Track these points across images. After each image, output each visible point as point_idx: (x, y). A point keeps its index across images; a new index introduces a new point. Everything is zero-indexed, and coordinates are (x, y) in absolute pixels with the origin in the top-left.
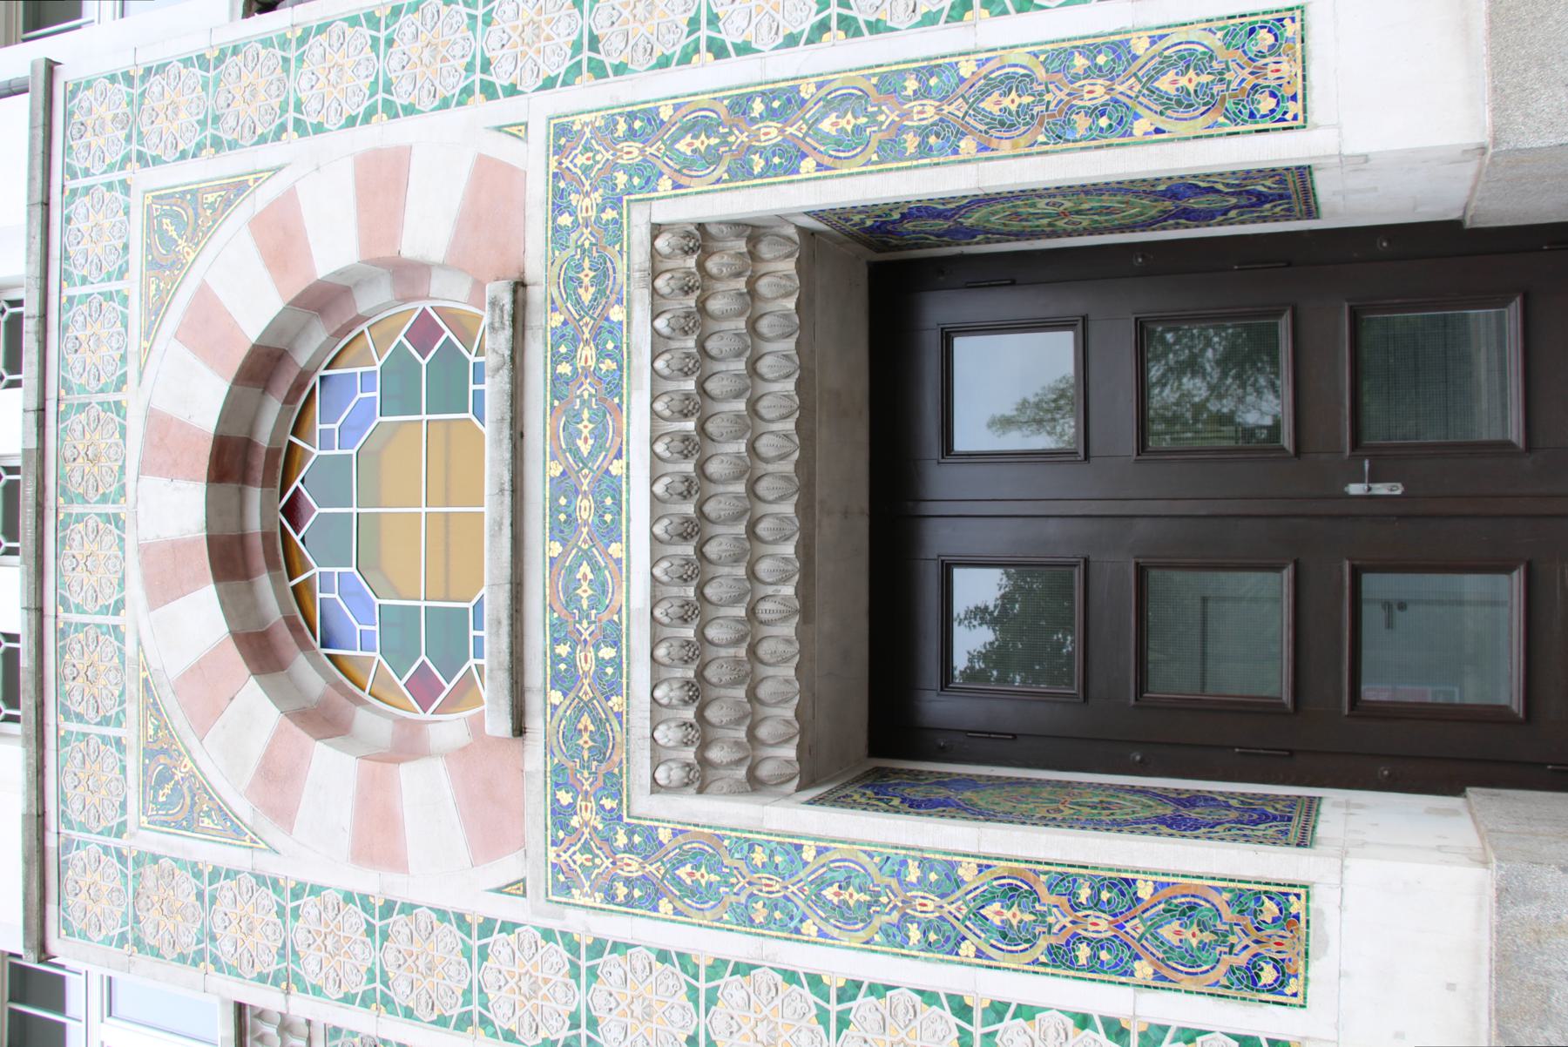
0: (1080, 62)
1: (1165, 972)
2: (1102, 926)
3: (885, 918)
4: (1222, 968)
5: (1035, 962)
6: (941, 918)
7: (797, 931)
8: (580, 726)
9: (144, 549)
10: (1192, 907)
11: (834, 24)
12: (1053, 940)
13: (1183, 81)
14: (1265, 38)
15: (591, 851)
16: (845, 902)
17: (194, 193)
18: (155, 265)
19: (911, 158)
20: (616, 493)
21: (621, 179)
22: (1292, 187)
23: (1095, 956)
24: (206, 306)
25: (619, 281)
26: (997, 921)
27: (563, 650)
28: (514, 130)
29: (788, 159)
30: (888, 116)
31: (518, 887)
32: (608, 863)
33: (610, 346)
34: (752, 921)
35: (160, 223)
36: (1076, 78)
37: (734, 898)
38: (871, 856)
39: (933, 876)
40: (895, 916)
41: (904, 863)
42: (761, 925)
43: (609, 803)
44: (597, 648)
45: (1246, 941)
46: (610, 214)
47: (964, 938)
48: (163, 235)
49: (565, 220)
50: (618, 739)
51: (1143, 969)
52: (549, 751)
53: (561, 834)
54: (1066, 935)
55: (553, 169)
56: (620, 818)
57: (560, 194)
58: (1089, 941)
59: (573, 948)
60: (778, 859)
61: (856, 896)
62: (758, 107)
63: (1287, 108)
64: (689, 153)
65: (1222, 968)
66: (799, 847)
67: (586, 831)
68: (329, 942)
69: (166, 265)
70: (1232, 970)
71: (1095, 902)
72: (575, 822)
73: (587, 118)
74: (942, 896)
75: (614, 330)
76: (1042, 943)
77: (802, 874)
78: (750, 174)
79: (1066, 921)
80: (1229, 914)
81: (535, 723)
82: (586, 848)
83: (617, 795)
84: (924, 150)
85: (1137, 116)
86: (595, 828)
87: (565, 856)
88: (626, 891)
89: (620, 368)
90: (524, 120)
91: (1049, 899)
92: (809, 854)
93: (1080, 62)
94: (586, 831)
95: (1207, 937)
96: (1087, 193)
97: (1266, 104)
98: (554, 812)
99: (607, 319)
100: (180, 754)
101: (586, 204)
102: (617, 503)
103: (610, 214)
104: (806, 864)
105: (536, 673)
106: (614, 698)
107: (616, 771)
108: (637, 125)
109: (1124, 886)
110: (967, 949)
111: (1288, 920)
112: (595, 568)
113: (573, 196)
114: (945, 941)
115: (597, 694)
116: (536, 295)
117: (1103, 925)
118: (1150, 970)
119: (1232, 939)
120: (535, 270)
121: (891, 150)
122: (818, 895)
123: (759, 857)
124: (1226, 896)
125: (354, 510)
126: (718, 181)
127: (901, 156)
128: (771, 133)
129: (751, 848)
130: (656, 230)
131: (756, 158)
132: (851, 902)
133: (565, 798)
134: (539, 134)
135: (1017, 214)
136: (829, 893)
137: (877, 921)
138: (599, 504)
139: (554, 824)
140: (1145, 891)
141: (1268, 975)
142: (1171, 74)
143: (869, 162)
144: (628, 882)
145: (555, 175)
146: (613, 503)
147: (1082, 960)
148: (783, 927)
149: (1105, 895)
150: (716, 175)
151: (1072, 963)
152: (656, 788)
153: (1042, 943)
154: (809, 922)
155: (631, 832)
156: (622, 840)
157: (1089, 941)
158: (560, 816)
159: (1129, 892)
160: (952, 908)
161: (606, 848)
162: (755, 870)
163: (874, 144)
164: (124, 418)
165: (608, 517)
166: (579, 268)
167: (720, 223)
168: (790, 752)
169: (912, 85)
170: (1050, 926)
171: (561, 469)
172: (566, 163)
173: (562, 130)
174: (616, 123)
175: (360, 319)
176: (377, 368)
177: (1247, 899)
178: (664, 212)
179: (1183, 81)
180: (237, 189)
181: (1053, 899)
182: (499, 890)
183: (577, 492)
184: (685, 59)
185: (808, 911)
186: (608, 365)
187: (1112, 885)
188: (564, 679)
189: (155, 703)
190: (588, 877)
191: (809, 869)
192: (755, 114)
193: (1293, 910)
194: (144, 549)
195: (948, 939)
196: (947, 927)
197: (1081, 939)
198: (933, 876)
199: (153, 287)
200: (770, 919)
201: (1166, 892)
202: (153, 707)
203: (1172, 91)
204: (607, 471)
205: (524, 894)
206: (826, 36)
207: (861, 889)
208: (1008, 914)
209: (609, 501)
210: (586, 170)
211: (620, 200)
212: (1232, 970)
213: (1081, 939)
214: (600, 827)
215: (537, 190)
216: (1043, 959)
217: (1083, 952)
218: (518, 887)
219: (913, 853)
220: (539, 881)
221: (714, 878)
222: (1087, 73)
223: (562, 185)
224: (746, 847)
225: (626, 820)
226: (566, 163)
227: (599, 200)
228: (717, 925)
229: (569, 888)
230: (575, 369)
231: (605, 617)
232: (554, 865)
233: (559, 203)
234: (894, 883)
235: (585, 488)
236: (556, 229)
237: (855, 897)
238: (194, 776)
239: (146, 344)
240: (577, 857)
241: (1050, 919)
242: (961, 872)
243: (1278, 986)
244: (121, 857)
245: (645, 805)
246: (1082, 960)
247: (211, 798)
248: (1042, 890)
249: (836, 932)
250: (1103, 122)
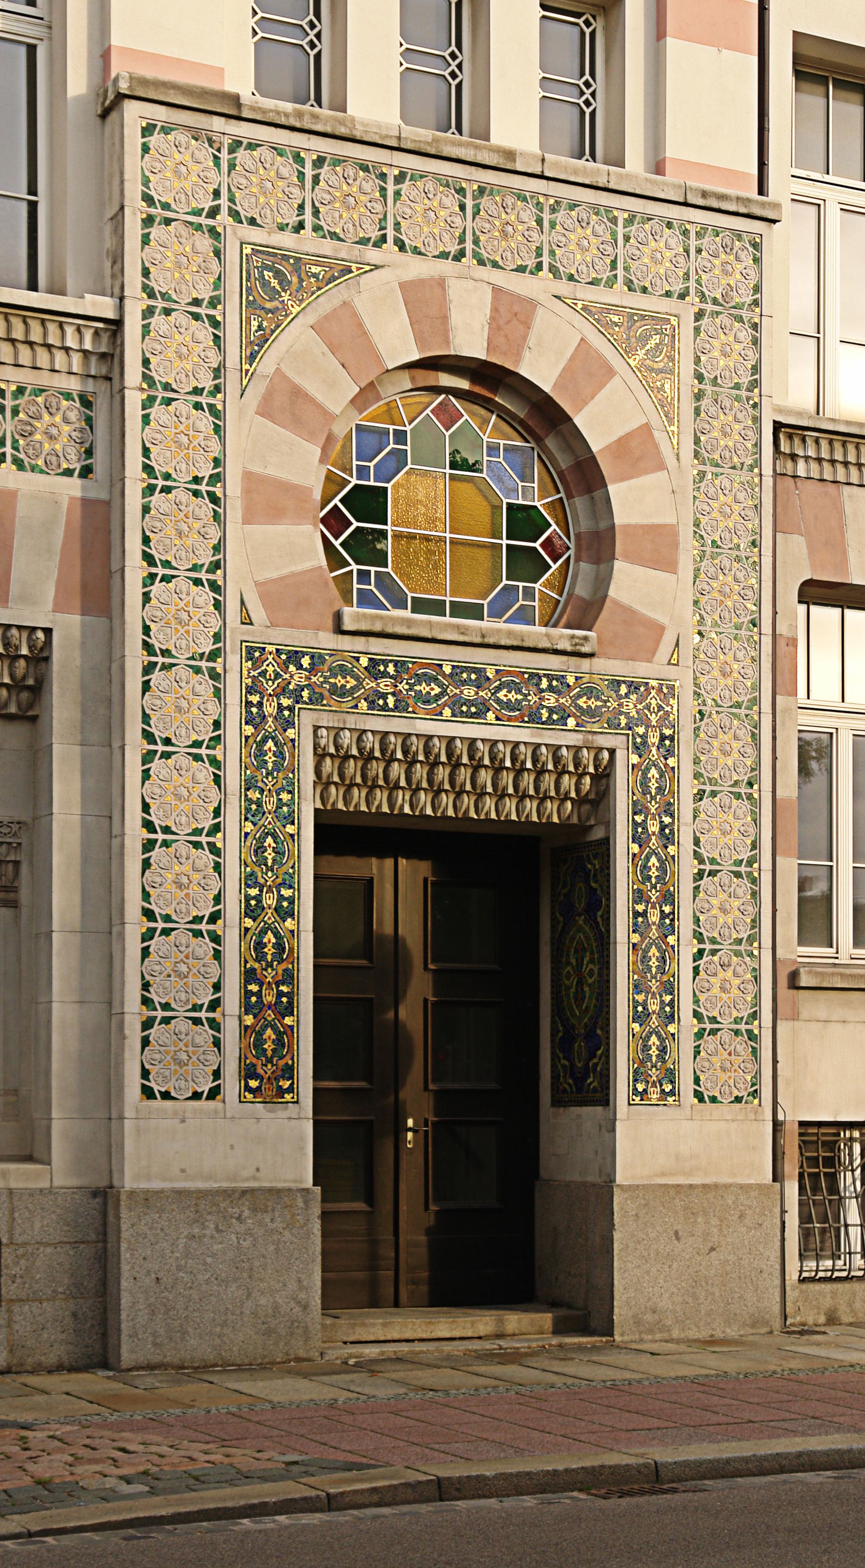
1: (249, 1031)
2: (269, 998)
3: (260, 874)
4: (254, 1061)
5: (246, 962)
6: (264, 908)
7: (246, 819)
10: (283, 1045)
11: (702, 867)
12: (259, 971)
13: (654, 1048)
14: (668, 1088)
15: (276, 679)
16: (266, 850)
17: (672, 372)
19: (634, 908)
21: (641, 730)
23: (253, 994)
25: (588, 725)
26: (265, 940)
27: (391, 669)
28: (675, 656)
29: (639, 837)
30: (654, 896)
32: (270, 691)
33: (555, 717)
34: (247, 789)
36: (661, 996)
37: (260, 778)
38: (293, 867)
39: (285, 904)
40: (262, 881)
41: (291, 887)
42: (246, 795)
43: (305, 693)
44: (393, 694)
45: (269, 1072)
46: (623, 721)
47: (254, 920)
49: (623, 689)
50: (343, 705)
51: (249, 1020)
52: (334, 652)
53: (284, 657)
54: (263, 978)
56: (298, 702)
58: (260, 991)
59: (213, 656)
60: (285, 809)
61: (270, 857)
65: (254, 1061)
66: (293, 823)
67: (287, 676)
68: (184, 439)
70: (254, 1065)
71: (280, 994)
72: (292, 668)
73: (675, 709)
74: (275, 909)
75: (563, 720)
76: (257, 965)
77: (278, 824)
78: (635, 813)
79: (269, 979)
80: (282, 1063)
81: (346, 643)
82: (277, 675)
83: (311, 701)
84: (637, 914)
85: (641, 1025)
86: (289, 683)
87: (270, 657)
88: (255, 702)
89: (543, 723)
91: (280, 969)
92: (290, 829)
93: (667, 998)
94: (287, 676)
95: (269, 1053)
96: (600, 994)
97: (640, 1087)
98: (296, 652)
99: (569, 716)
100: (301, 301)
102: (473, 715)
103: (623, 721)
104: (284, 826)
105: (377, 646)
106: (365, 704)
107: (325, 702)
108: (667, 742)
109: (290, 1010)
110: (249, 923)
111: (281, 1092)
112: (438, 697)
114: (252, 910)
115: (367, 693)
116: (585, 664)
117: (269, 999)
118: (249, 1023)
119: (269, 1066)
120: (600, 664)
121: (639, 896)
122: (267, 834)
123: (285, 797)
124: (290, 1062)
126: (633, 794)
127: (635, 902)
128: (654, 827)
129: (290, 792)
130: (612, 752)
131: (642, 818)
132: (266, 854)
133: (306, 662)
134: (671, 672)
135: (584, 950)
136: (269, 840)
137: (257, 869)
138: (469, 703)
139: (289, 651)
140: (288, 1021)
141: (253, 1084)
143: (633, 883)
144: (260, 704)
146: (477, 719)
147: (250, 987)
148: (248, 810)
149: (284, 1000)
150: (636, 792)
151: (247, 982)
152: (316, 728)
153: (257, 965)
155: (291, 709)
156: (286, 702)
157: (260, 991)
158: (294, 657)
160: (269, 915)
161: (279, 690)
162: (278, 794)
163: (642, 887)
165: (464, 708)
166: (598, 698)
167: (608, 786)
169: (667, 909)
170: (266, 970)
171: (491, 676)
175: (569, 496)
178: (620, 755)
179: (654, 1048)
181: (280, 972)
183: (478, 687)
185: (258, 827)
186: (545, 714)
187: (290, 1003)
188: (374, 668)
189: (335, 279)
190: (259, 674)
191: (282, 828)
193: (286, 1095)
195: (252, 911)
196: (259, 911)
197: (261, 987)
198: (285, 904)
199: (615, 319)
200: (249, 801)
201: (289, 1032)
203: (650, 1043)
204: (489, 710)
205: (243, 623)
206: (696, 862)
207: (274, 860)
208: (270, 946)
209: (473, 709)
210: (648, 707)
211: (630, 729)
212: (254, 1065)
213: (261, 987)
214: (291, 687)
215: (639, 670)
216: (248, 966)
217: (254, 988)
218: (247, 621)
221: (270, 766)
222: (662, 1002)
223: (642, 689)
224: (290, 788)
225: (297, 706)
226: (653, 692)
228: (243, 766)
229: (251, 659)
230: (542, 691)
231: (411, 702)
232: (264, 649)
233: (633, 687)
234: (279, 880)
235: (481, 693)
236: (619, 683)
237: (270, 855)
238: (287, 316)
240: (270, 669)
241: (270, 970)
242: (289, 920)
243: (248, 1088)
244: (214, 212)
245: (307, 719)
246: (250, 987)
247: (273, 331)
248: (284, 966)
249: (248, 844)
250: (640, 1009)
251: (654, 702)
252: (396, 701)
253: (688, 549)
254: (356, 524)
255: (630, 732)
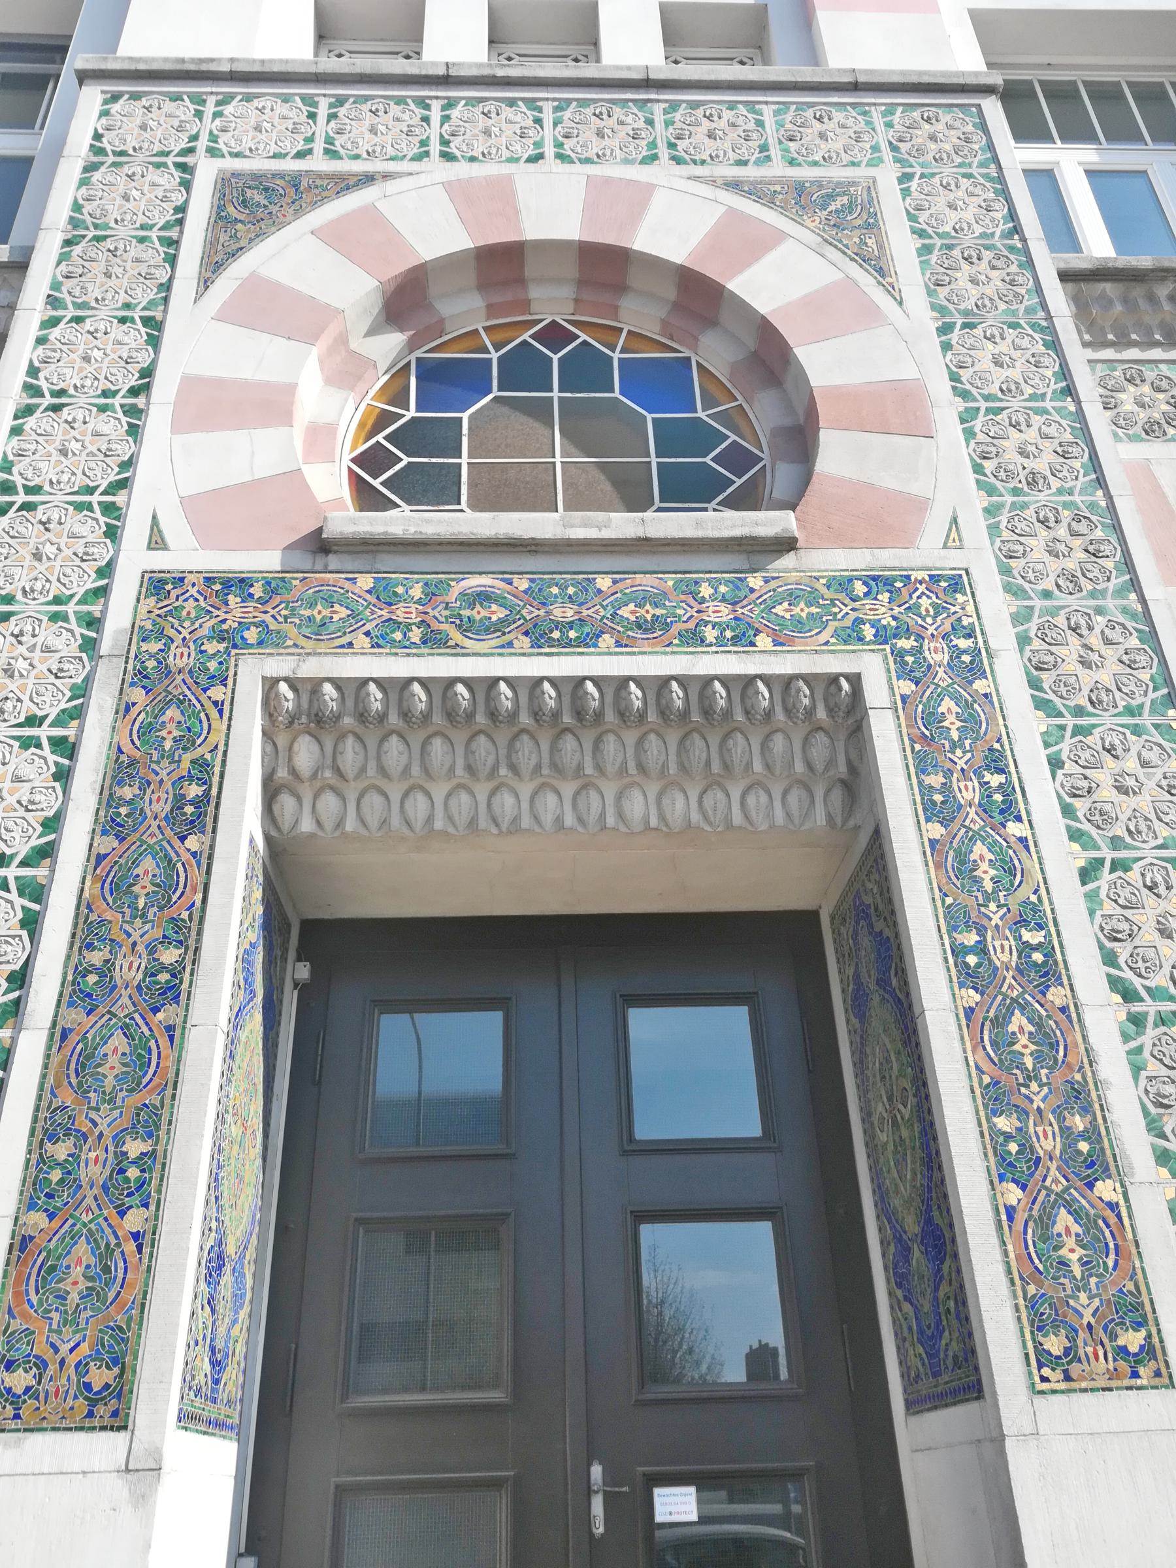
0: (1079, 1123)
8: (337, 607)
9: (510, 178)
18: (800, 189)
20: (582, 642)
22: (957, 1376)
24: (760, 243)
31: (157, 541)
35: (844, 193)
46: (869, 632)
48: (831, 197)
55: (914, 575)
56: (235, 646)
57: (888, 582)
62: (995, 780)
63: (1056, 1369)
64: (940, 710)
69: (800, 198)
73: (970, 608)
86: (224, 621)
90: (966, 543)
101: (883, 610)
103: (869, 632)
113: (887, 595)
116: (787, 561)
125: (556, 394)
134: (952, 561)
138: (571, 626)
142: (1076, 1228)
145: (908, 577)
152: (270, 684)
154: (116, 844)
159: (136, 1200)
164: (641, 163)
168: (307, 825)
172: (922, 588)
173: (956, 585)
174: (969, 636)
176: (701, 414)
177: (119, 1351)
180: (880, 270)
182: (154, 517)
184: (1041, 704)
192: (987, 777)
194: (510, 178)
202: (345, 184)
210: (913, 609)
218: (157, 541)
219: (191, 953)
220: (160, 561)
225: (233, 652)
227: (884, 622)
233: (877, 582)
239: (720, 181)
251: (924, 602)
252: (424, 635)
253: (946, 411)
254: (406, 460)
255: (887, 647)
